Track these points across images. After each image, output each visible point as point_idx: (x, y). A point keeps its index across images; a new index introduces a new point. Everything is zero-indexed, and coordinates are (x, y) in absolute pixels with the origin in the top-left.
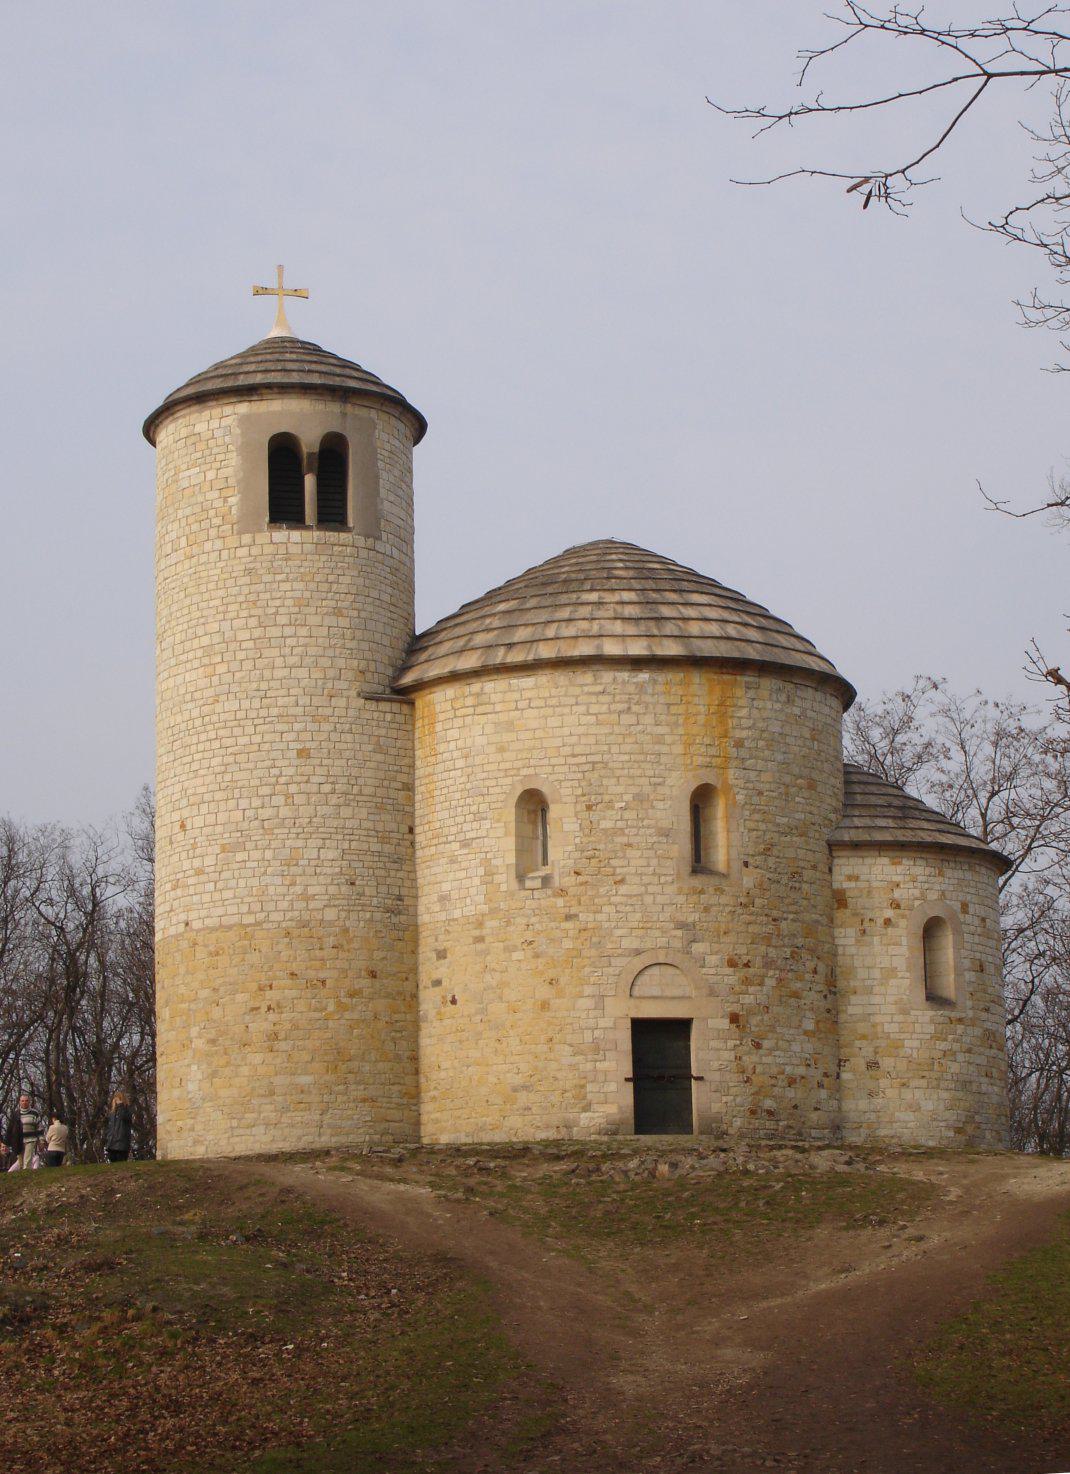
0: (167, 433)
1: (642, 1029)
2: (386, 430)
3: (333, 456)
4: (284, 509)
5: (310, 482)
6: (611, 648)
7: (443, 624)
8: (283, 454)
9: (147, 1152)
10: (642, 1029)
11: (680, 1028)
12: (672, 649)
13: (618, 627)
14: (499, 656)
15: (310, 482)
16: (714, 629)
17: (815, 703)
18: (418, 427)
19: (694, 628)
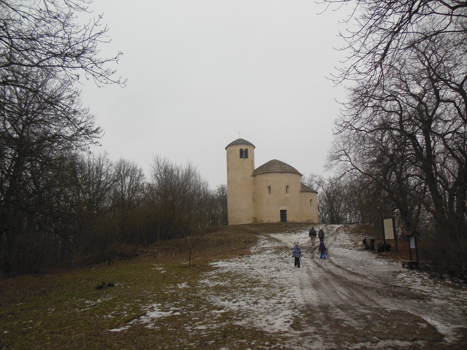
0: (228, 148)
1: (282, 211)
2: (252, 148)
3: (246, 150)
4: (241, 156)
5: (244, 154)
6: (277, 171)
7: (258, 169)
8: (241, 151)
9: (227, 224)
10: (282, 211)
11: (285, 211)
12: (284, 171)
13: (278, 169)
14: (265, 172)
15: (244, 154)
16: (288, 169)
17: (298, 176)
18: (254, 147)
19: (286, 169)
